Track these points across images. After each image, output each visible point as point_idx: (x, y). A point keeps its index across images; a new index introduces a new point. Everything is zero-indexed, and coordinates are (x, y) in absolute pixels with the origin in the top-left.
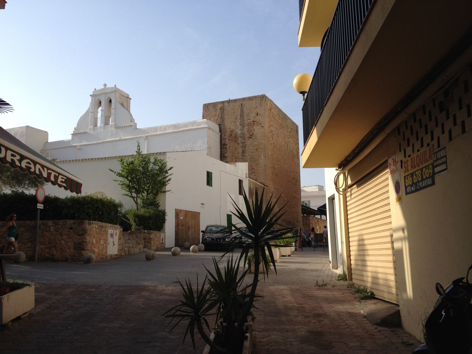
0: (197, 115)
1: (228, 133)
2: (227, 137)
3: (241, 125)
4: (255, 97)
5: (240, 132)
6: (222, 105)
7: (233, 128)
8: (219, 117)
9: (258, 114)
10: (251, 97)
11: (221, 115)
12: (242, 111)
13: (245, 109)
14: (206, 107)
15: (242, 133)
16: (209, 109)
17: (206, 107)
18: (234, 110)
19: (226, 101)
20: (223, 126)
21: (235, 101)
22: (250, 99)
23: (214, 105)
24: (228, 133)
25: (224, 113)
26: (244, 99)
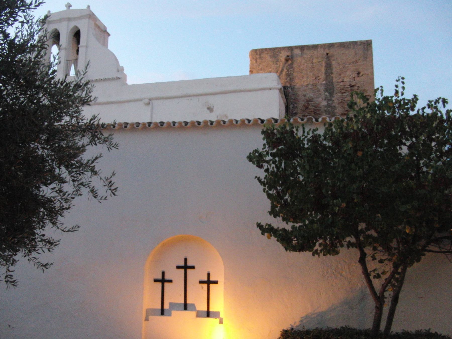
0: (241, 67)
1: (301, 104)
2: (299, 111)
3: (326, 90)
4: (355, 43)
5: (324, 103)
6: (289, 54)
7: (310, 95)
8: (284, 73)
9: (359, 73)
10: (346, 43)
11: (288, 71)
12: (329, 66)
13: (334, 63)
14: (258, 55)
15: (329, 106)
16: (261, 57)
17: (258, 55)
18: (312, 63)
19: (296, 47)
20: (290, 90)
21: (315, 47)
22: (343, 45)
23: (274, 52)
24: (301, 104)
25: (292, 67)
26: (331, 45)
